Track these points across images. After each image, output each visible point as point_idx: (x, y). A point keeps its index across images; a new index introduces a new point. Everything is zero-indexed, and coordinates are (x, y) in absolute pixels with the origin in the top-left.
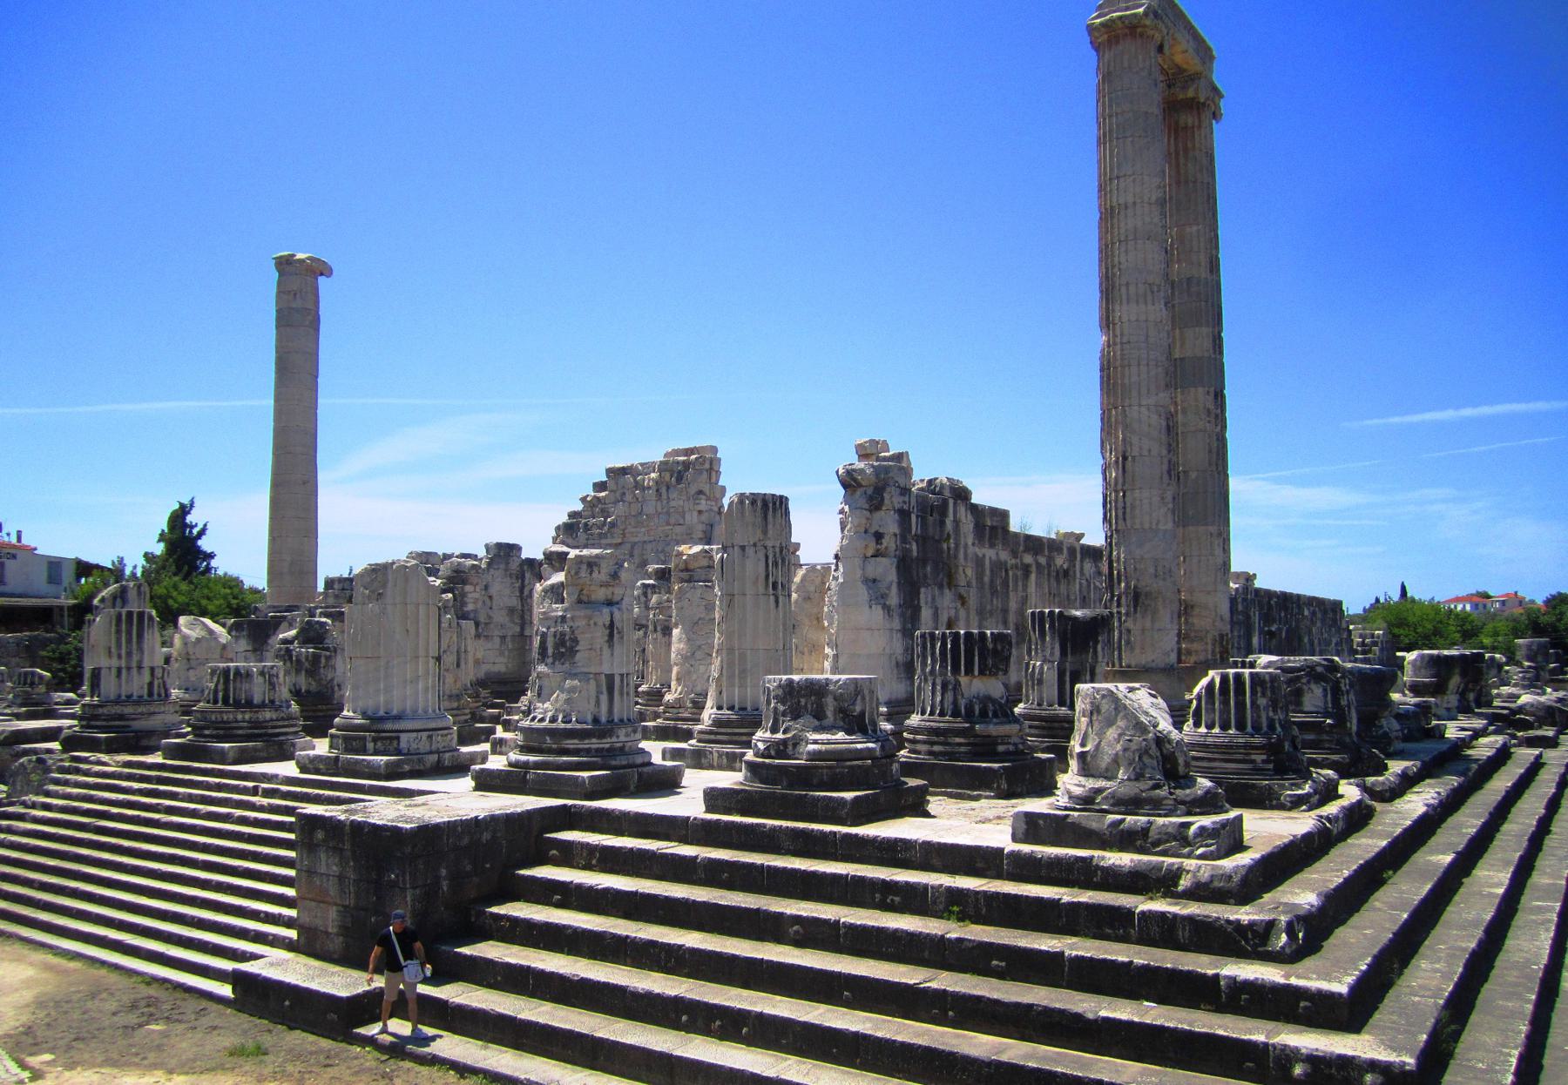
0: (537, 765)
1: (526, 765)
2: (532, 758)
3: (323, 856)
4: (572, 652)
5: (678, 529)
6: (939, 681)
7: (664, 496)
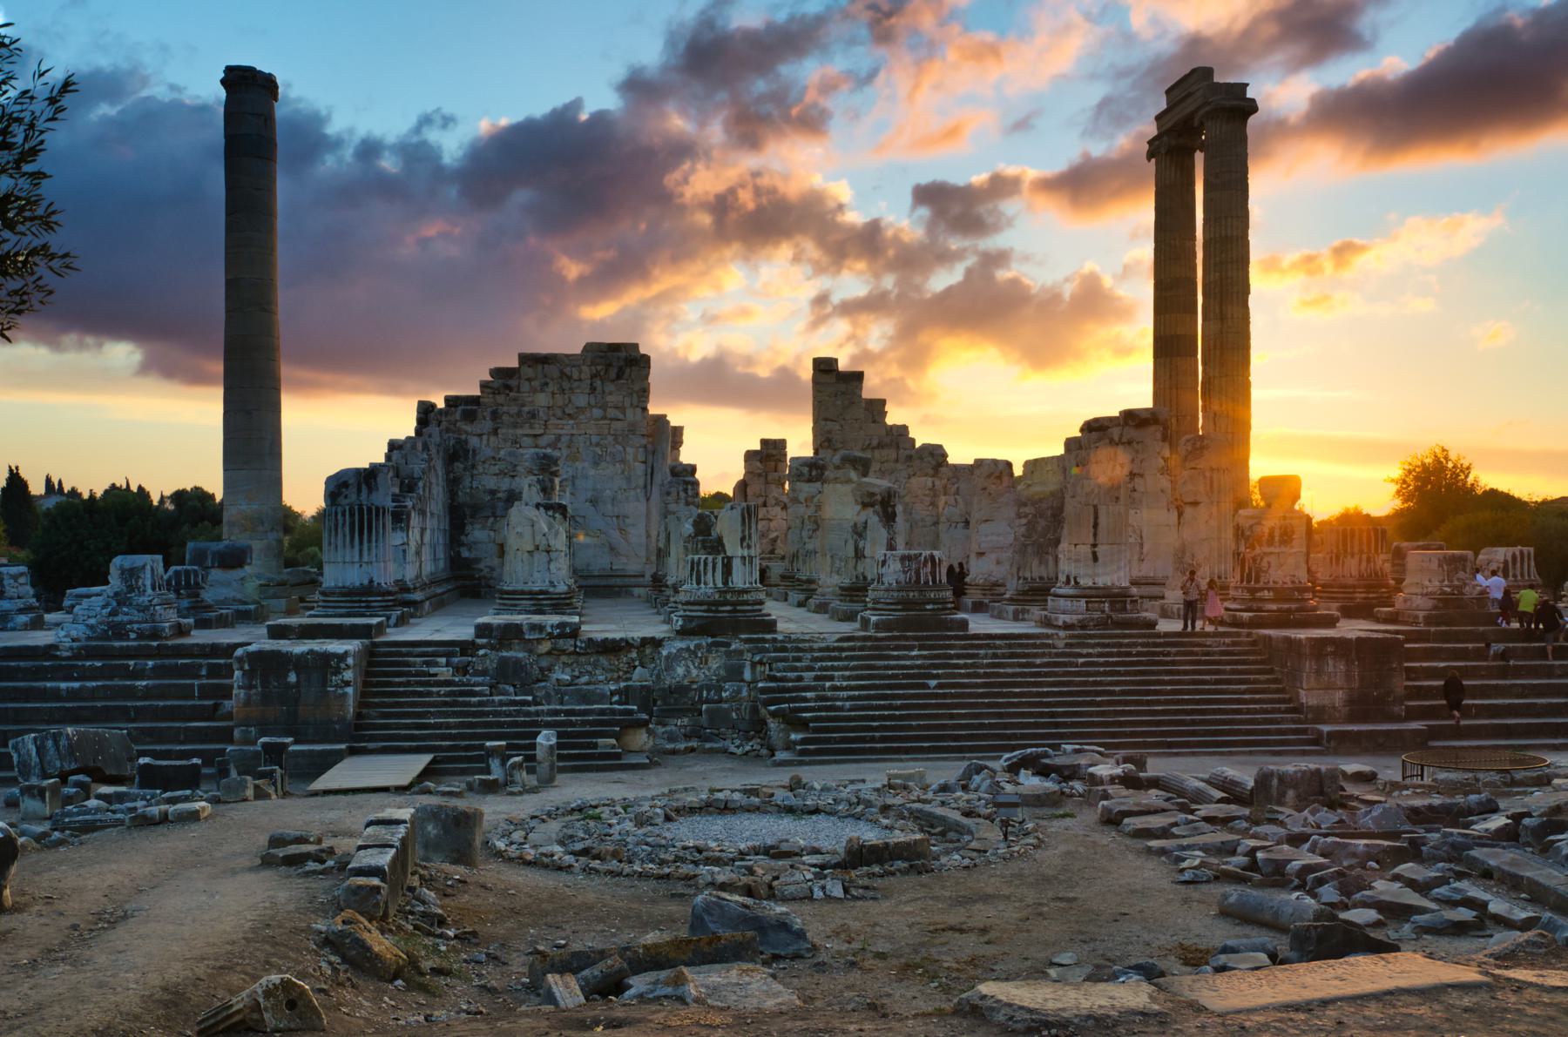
0: (1298, 610)
1: (1289, 611)
2: (1293, 606)
3: (1330, 662)
4: (1292, 540)
5: (617, 425)
6: (1364, 557)
7: (599, 389)
